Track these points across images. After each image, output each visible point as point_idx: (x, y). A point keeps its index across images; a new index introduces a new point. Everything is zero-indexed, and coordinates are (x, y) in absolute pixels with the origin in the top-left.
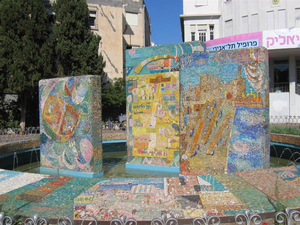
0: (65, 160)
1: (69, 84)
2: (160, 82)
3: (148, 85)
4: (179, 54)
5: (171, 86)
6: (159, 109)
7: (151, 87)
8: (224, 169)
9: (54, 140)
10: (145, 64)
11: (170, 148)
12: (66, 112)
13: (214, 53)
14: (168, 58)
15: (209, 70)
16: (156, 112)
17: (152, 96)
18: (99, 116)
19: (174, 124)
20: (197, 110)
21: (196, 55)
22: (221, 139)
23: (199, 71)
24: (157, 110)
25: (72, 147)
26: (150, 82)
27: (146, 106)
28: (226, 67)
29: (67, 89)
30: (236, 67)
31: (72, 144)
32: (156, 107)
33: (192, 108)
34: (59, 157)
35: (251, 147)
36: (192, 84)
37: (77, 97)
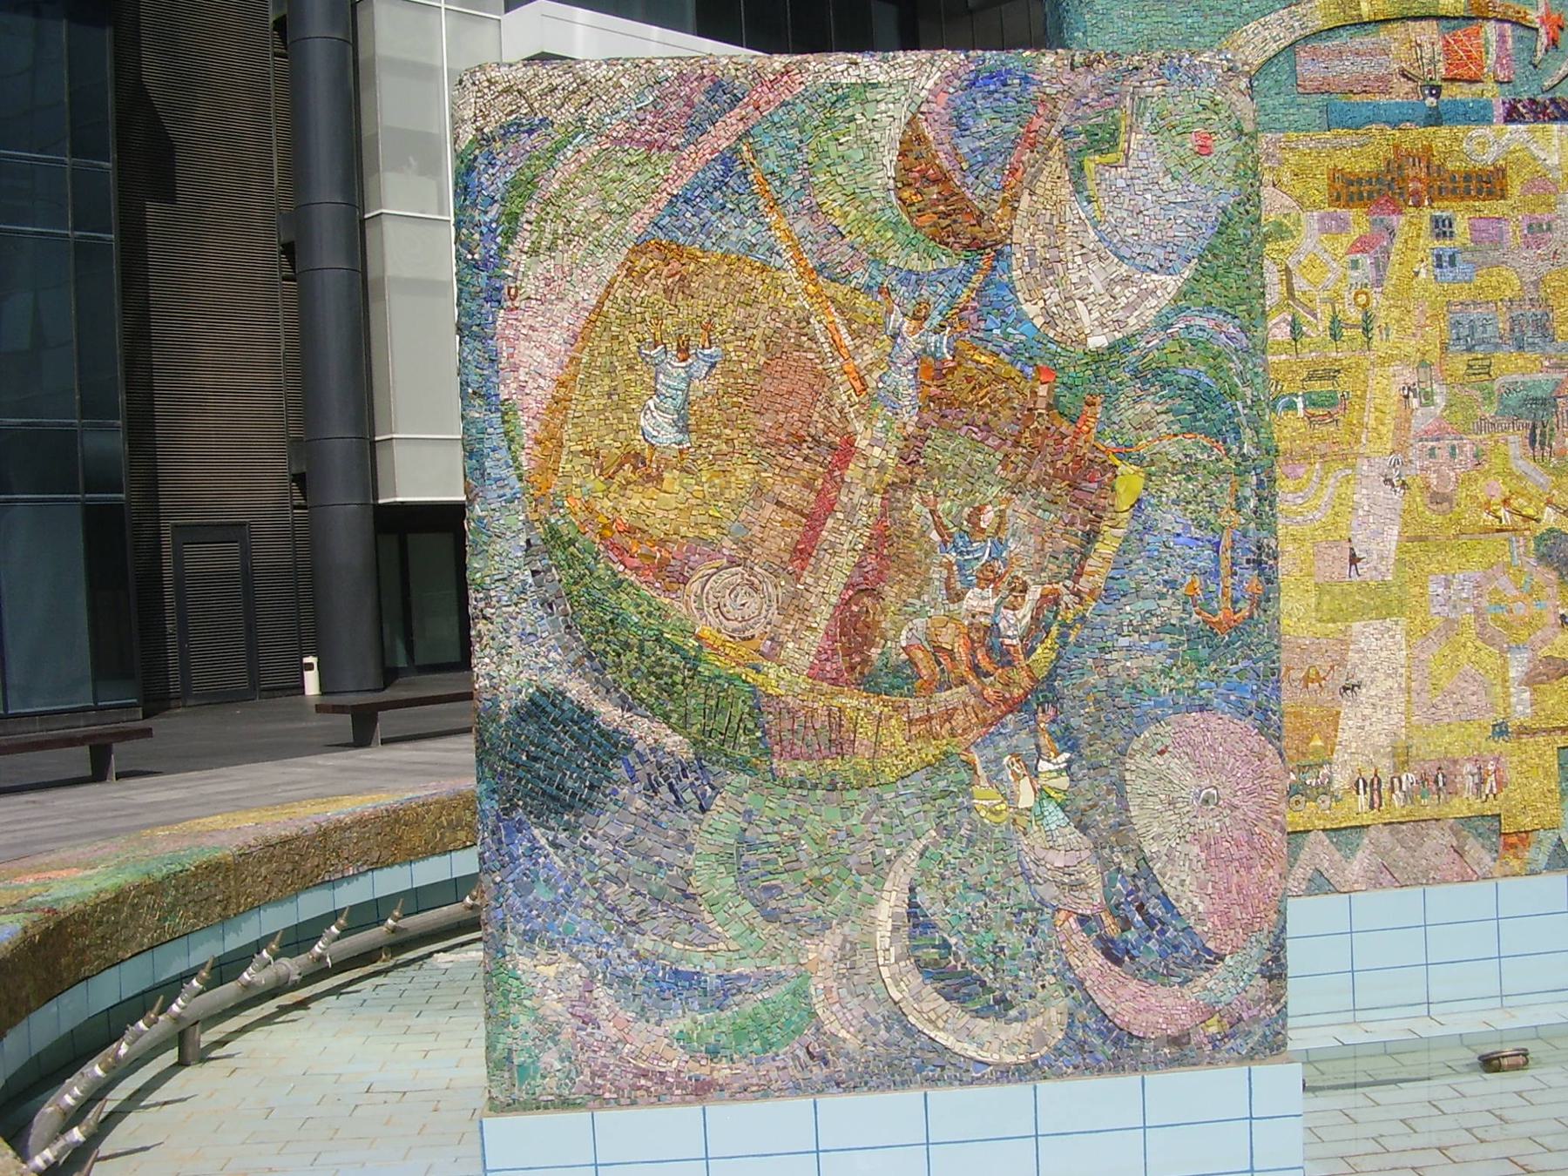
0: (916, 979)
1: (963, 129)
2: (1418, 205)
5: (1513, 232)
6: (1423, 418)
7: (1346, 240)
9: (744, 766)
10: (1273, 48)
11: (1524, 731)
16: (1401, 447)
17: (1355, 315)
19: (1551, 530)
24: (1403, 424)
25: (1019, 821)
26: (1336, 200)
27: (1300, 403)
31: (1025, 793)
32: (1393, 407)
34: (821, 951)
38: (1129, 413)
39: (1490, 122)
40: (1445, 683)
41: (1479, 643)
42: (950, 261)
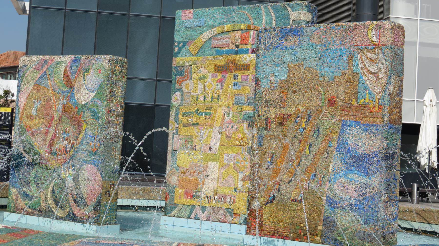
2: (231, 72)
3: (210, 75)
4: (268, 22)
6: (227, 119)
7: (216, 80)
8: (317, 227)
12: (61, 116)
13: (312, 28)
14: (249, 28)
15: (304, 57)
16: (222, 125)
17: (216, 96)
18: (118, 127)
20: (281, 124)
21: (285, 30)
22: (315, 175)
23: (287, 57)
24: (223, 120)
28: (329, 53)
29: (68, 76)
30: (345, 54)
32: (221, 116)
33: (272, 120)
35: (361, 191)
36: (275, 79)
37: (83, 92)
38: (86, 115)
39: (248, 53)
40: (226, 178)
41: (233, 170)
42: (67, 89)
